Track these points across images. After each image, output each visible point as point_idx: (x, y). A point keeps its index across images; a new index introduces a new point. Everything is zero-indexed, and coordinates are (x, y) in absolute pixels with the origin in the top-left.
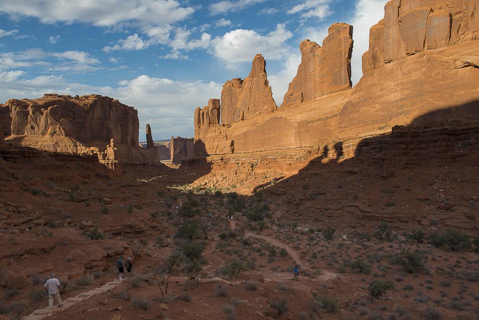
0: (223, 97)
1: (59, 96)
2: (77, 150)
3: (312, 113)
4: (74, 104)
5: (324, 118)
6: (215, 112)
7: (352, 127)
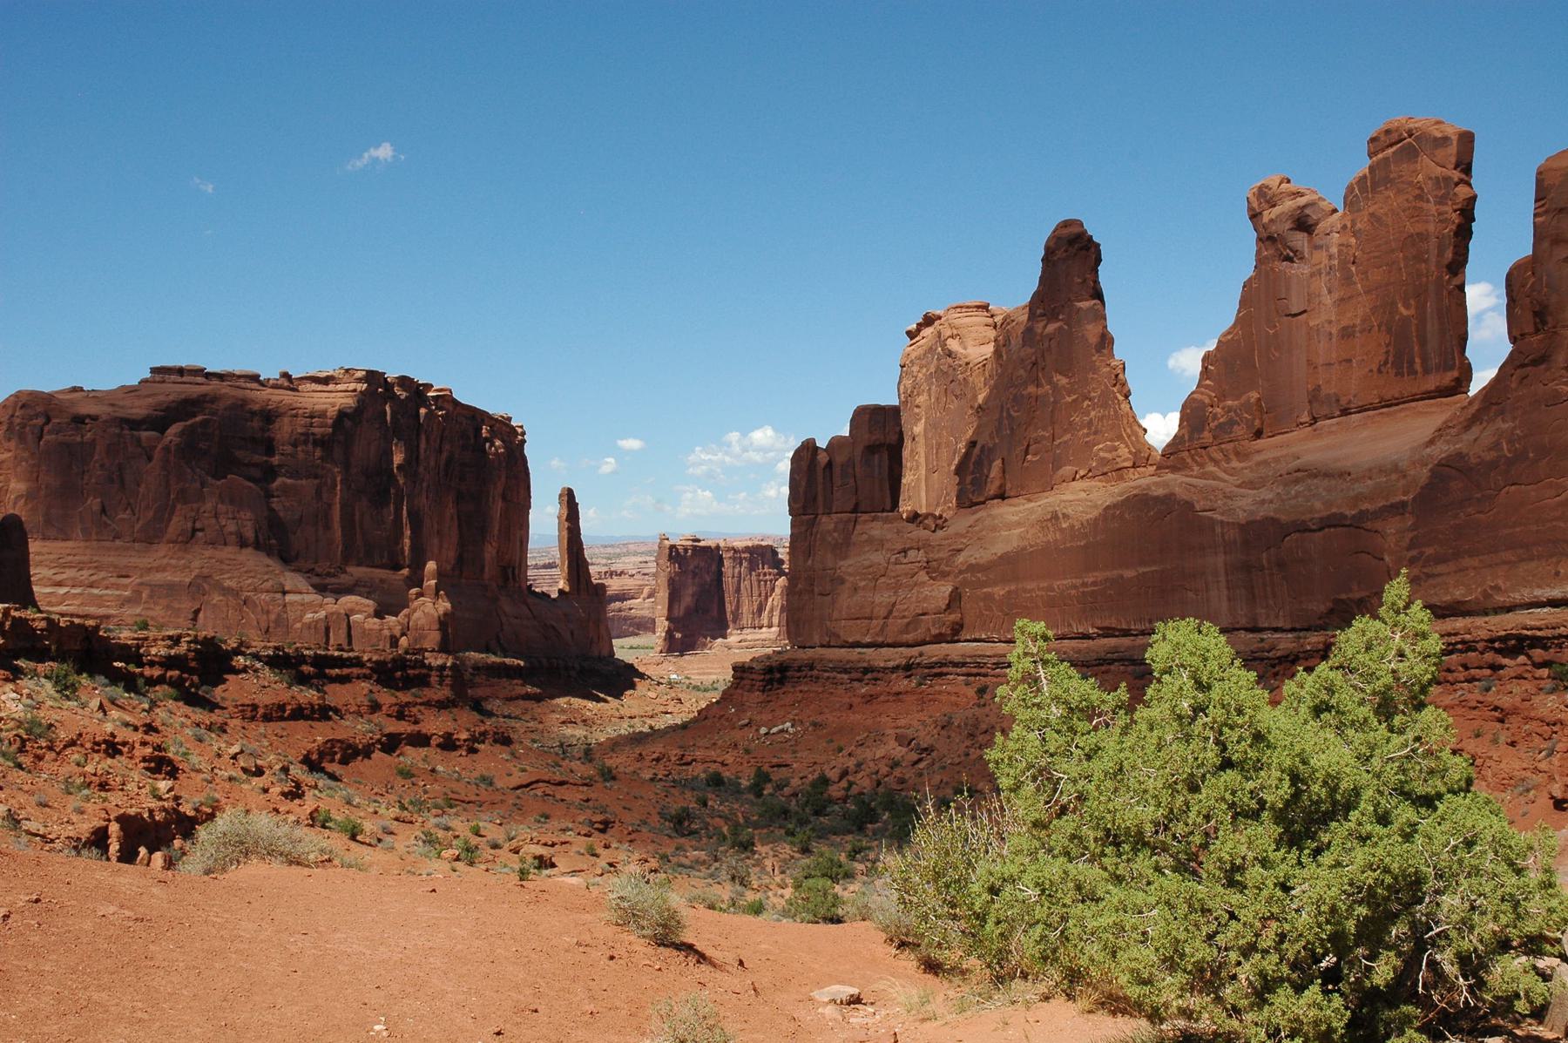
0: (908, 382)
1: (209, 376)
2: (285, 606)
3: (1299, 488)
4: (269, 416)
5: (1350, 513)
6: (881, 460)
7: (1467, 562)
